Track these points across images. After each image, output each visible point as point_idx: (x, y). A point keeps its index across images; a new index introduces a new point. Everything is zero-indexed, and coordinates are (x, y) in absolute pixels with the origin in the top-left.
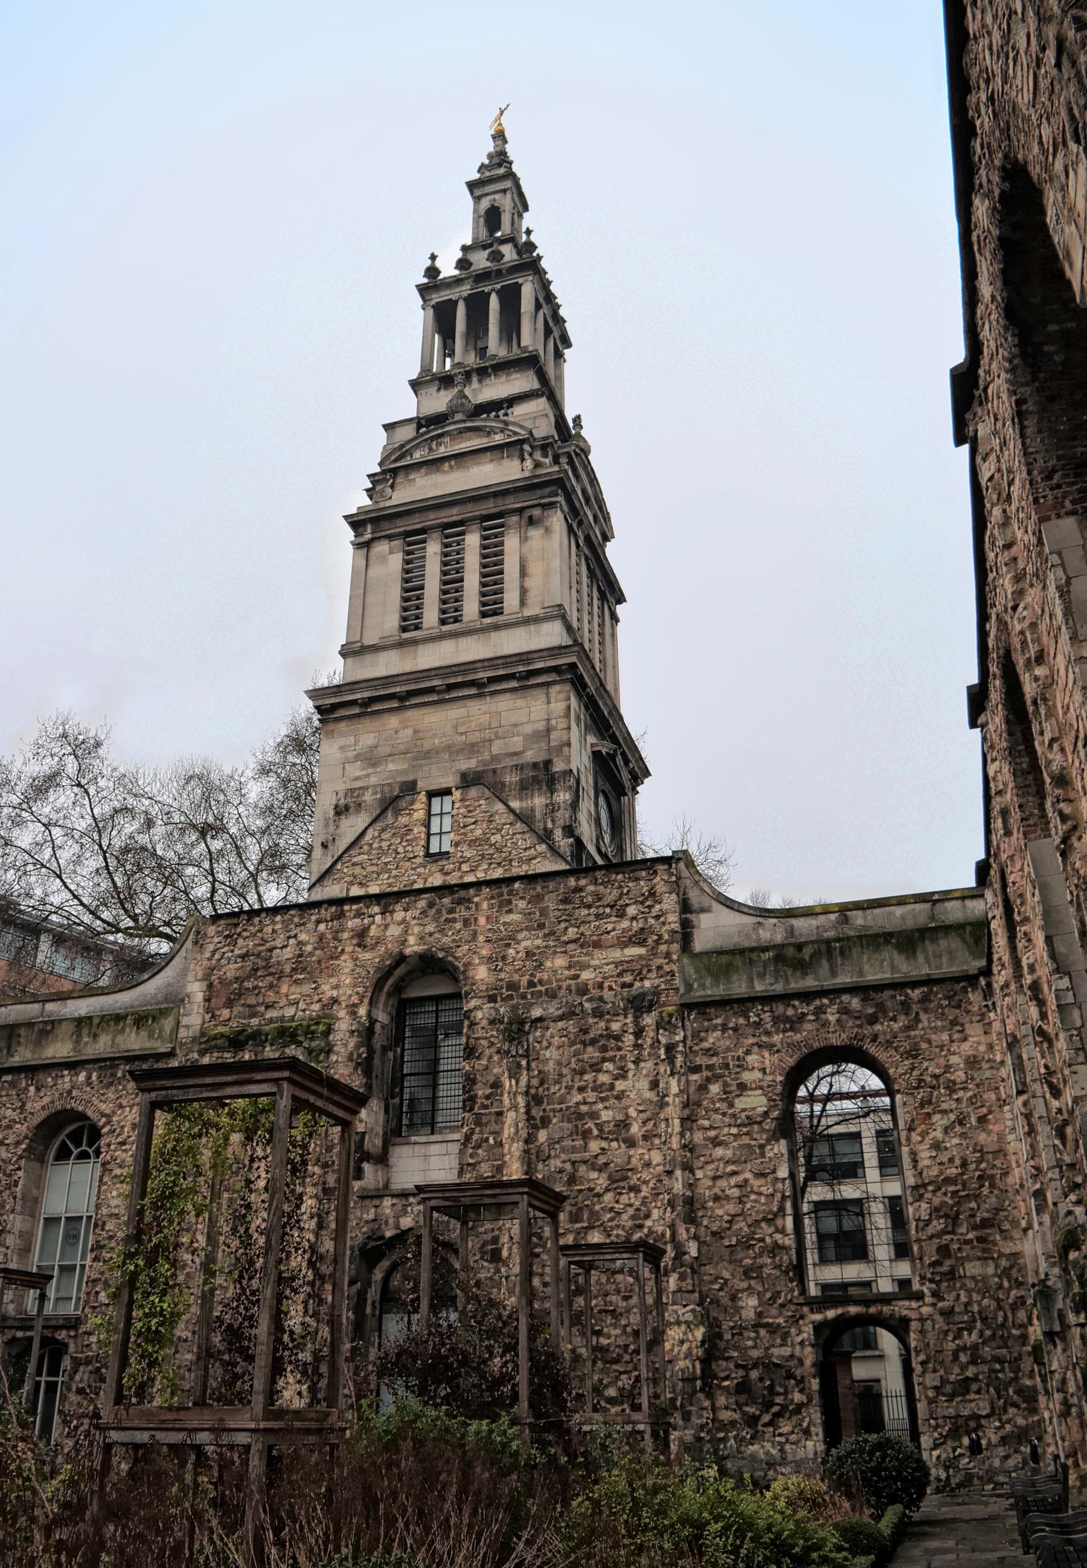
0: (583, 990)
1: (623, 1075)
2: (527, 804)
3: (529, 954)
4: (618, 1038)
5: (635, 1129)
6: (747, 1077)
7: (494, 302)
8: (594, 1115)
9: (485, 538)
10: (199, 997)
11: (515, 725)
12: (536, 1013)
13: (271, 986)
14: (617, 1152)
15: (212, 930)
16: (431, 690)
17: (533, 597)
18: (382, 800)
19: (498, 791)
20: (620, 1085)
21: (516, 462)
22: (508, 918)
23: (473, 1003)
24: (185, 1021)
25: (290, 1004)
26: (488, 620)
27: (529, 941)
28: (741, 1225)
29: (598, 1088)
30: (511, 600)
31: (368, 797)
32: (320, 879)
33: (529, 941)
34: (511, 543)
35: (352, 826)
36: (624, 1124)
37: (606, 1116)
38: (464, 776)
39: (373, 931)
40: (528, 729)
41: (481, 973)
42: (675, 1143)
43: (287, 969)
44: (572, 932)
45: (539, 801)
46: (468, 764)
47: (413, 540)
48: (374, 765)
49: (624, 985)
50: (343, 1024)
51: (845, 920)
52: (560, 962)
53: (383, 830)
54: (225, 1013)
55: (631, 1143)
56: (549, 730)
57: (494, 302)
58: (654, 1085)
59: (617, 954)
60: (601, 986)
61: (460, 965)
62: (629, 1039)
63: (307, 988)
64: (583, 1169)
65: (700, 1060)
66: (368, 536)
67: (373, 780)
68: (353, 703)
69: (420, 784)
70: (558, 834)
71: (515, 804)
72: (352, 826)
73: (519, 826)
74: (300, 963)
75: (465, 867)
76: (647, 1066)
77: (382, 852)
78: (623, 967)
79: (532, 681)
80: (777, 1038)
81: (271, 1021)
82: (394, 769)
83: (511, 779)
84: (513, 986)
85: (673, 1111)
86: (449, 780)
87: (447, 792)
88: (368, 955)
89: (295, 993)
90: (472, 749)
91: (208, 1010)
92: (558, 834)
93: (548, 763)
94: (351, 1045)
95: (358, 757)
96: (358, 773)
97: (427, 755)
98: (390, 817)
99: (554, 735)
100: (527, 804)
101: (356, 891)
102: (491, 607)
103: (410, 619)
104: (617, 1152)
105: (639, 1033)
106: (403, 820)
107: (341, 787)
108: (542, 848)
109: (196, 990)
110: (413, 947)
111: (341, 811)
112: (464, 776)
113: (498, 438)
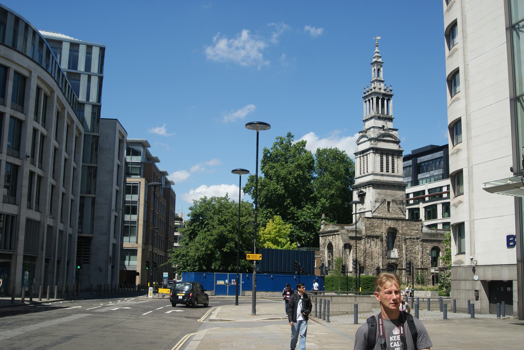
0: (411, 235)
1: (415, 247)
2: (400, 206)
3: (406, 230)
4: (415, 242)
5: (417, 253)
6: (428, 248)
7: (385, 101)
8: (412, 251)
9: (392, 158)
10: (364, 229)
11: (399, 194)
12: (407, 238)
13: (374, 229)
14: (415, 255)
15: (365, 219)
16: (388, 185)
17: (399, 171)
18: (382, 201)
19: (397, 204)
20: (415, 248)
21: (396, 145)
22: (403, 225)
23: (399, 235)
24: (363, 232)
25: (377, 232)
26: (393, 174)
27: (405, 228)
28: (426, 265)
29: (413, 248)
30: (396, 171)
31: (379, 200)
32: (374, 212)
33: (405, 228)
34: (396, 160)
35: (378, 204)
36: (415, 252)
37: (414, 251)
38: (392, 200)
39: (387, 223)
40: (400, 195)
41: (400, 231)
42: (421, 255)
43: (376, 226)
44: (410, 228)
45: (402, 206)
46: (393, 198)
47: (382, 155)
48: (380, 195)
49: (416, 236)
50: (384, 236)
51: (437, 231)
52: (409, 231)
53: (382, 206)
54: (368, 232)
55: (416, 255)
56: (403, 196)
57: (385, 101)
58: (419, 248)
59: (415, 232)
60: (413, 235)
61: (398, 230)
62: (416, 242)
63: (379, 230)
64: (411, 257)
65: (423, 246)
66: (375, 152)
67: (380, 198)
68: (377, 184)
69: (386, 200)
70: (404, 212)
71: (399, 206)
72: (378, 204)
73: (399, 210)
74: (378, 226)
75: (393, 214)
76: (418, 246)
77: (382, 210)
78: (416, 233)
79: (401, 187)
80: (430, 244)
81: (374, 234)
82: (383, 196)
83: (398, 202)
84: (404, 234)
85: (421, 252)
86: (390, 200)
87: (390, 202)
88: (386, 226)
89: (377, 230)
90: (393, 196)
91: (366, 231)
92: (404, 212)
93: (403, 201)
94: (385, 238)
95: (378, 193)
96: (378, 196)
97: (387, 195)
98: (383, 204)
99: (404, 197)
100: (400, 206)
101: (379, 215)
102: (393, 172)
103: (382, 171)
104: (415, 255)
105: (417, 242)
106: (384, 205)
107: (376, 198)
108: (402, 213)
109: (364, 228)
110: (392, 226)
111: (376, 202)
112: (392, 200)
113: (393, 139)
